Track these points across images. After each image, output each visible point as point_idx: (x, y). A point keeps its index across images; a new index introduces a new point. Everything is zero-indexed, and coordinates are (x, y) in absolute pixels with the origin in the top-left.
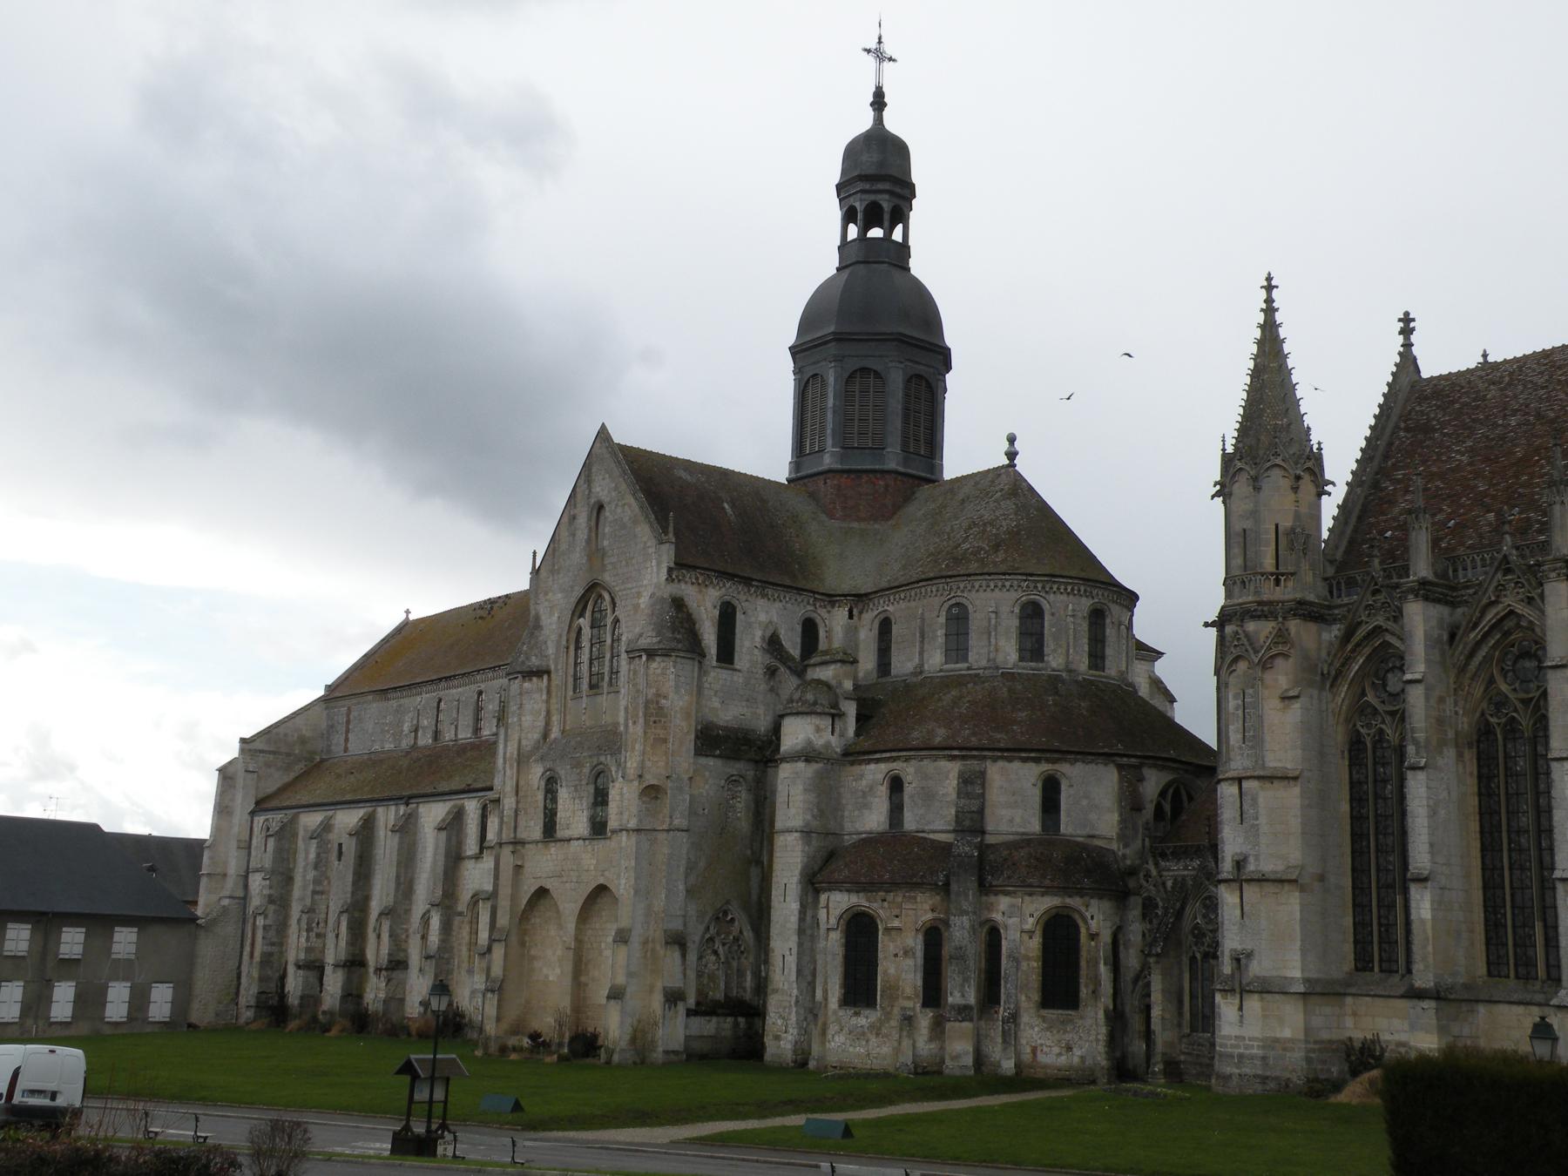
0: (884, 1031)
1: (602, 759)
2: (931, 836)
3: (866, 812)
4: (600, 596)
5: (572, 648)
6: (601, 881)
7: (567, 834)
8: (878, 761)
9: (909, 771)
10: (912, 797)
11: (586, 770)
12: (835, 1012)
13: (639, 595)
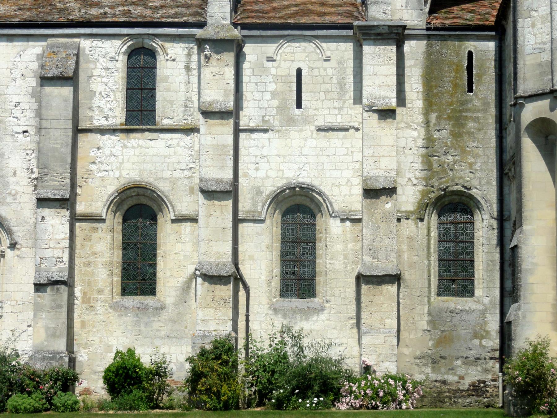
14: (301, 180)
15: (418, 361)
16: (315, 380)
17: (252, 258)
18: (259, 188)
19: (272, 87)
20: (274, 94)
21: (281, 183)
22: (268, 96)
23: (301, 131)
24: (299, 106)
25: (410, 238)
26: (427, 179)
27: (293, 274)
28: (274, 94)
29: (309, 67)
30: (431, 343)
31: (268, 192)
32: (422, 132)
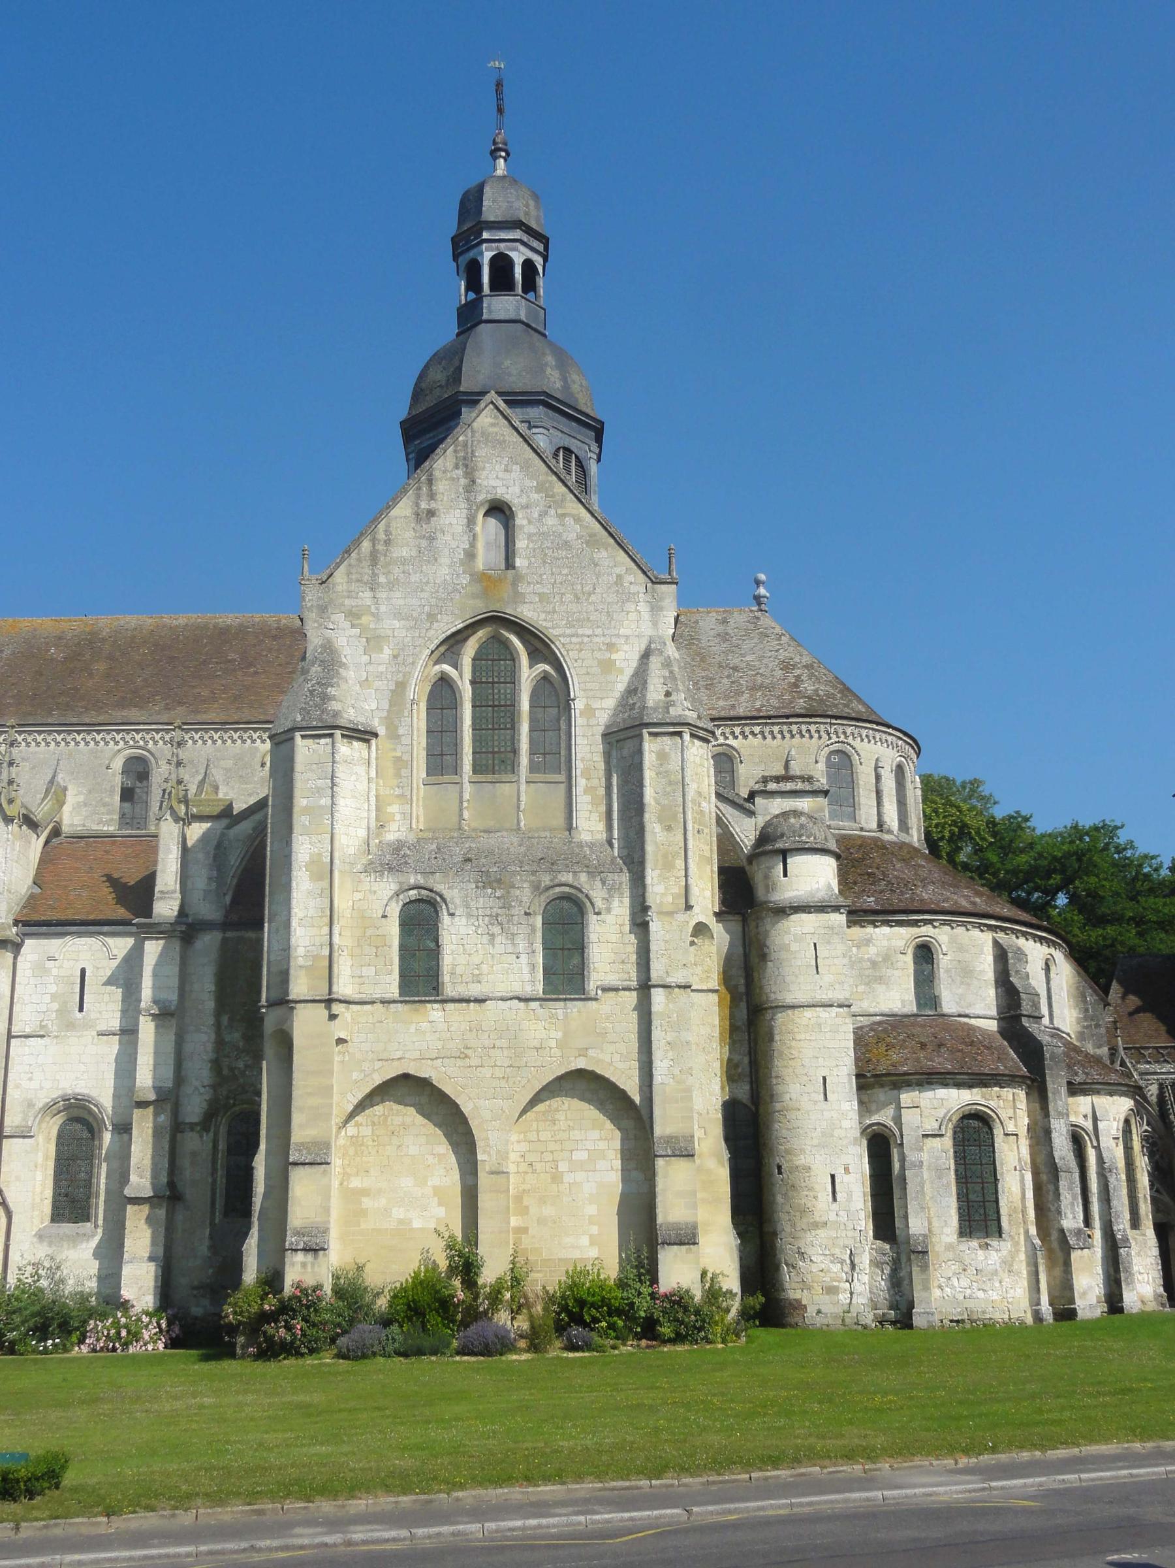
0: (1015, 1267)
1: (567, 878)
2: (973, 1022)
3: (880, 989)
4: (497, 639)
5: (423, 706)
6: (581, 1064)
7: (474, 990)
8: (900, 923)
9: (942, 936)
10: (948, 971)
11: (524, 892)
12: (950, 1247)
13: (611, 647)
14: (77, 1091)
15: (195, 1292)
16: (53, 1318)
17: (18, 1179)
18: (31, 1100)
19: (53, 989)
20: (54, 997)
21: (55, 1094)
22: (47, 999)
23: (81, 1036)
24: (81, 1009)
25: (194, 1154)
26: (214, 1087)
27: (66, 1195)
28: (54, 997)
29: (94, 967)
30: (211, 1271)
31: (41, 1105)
32: (213, 1036)
